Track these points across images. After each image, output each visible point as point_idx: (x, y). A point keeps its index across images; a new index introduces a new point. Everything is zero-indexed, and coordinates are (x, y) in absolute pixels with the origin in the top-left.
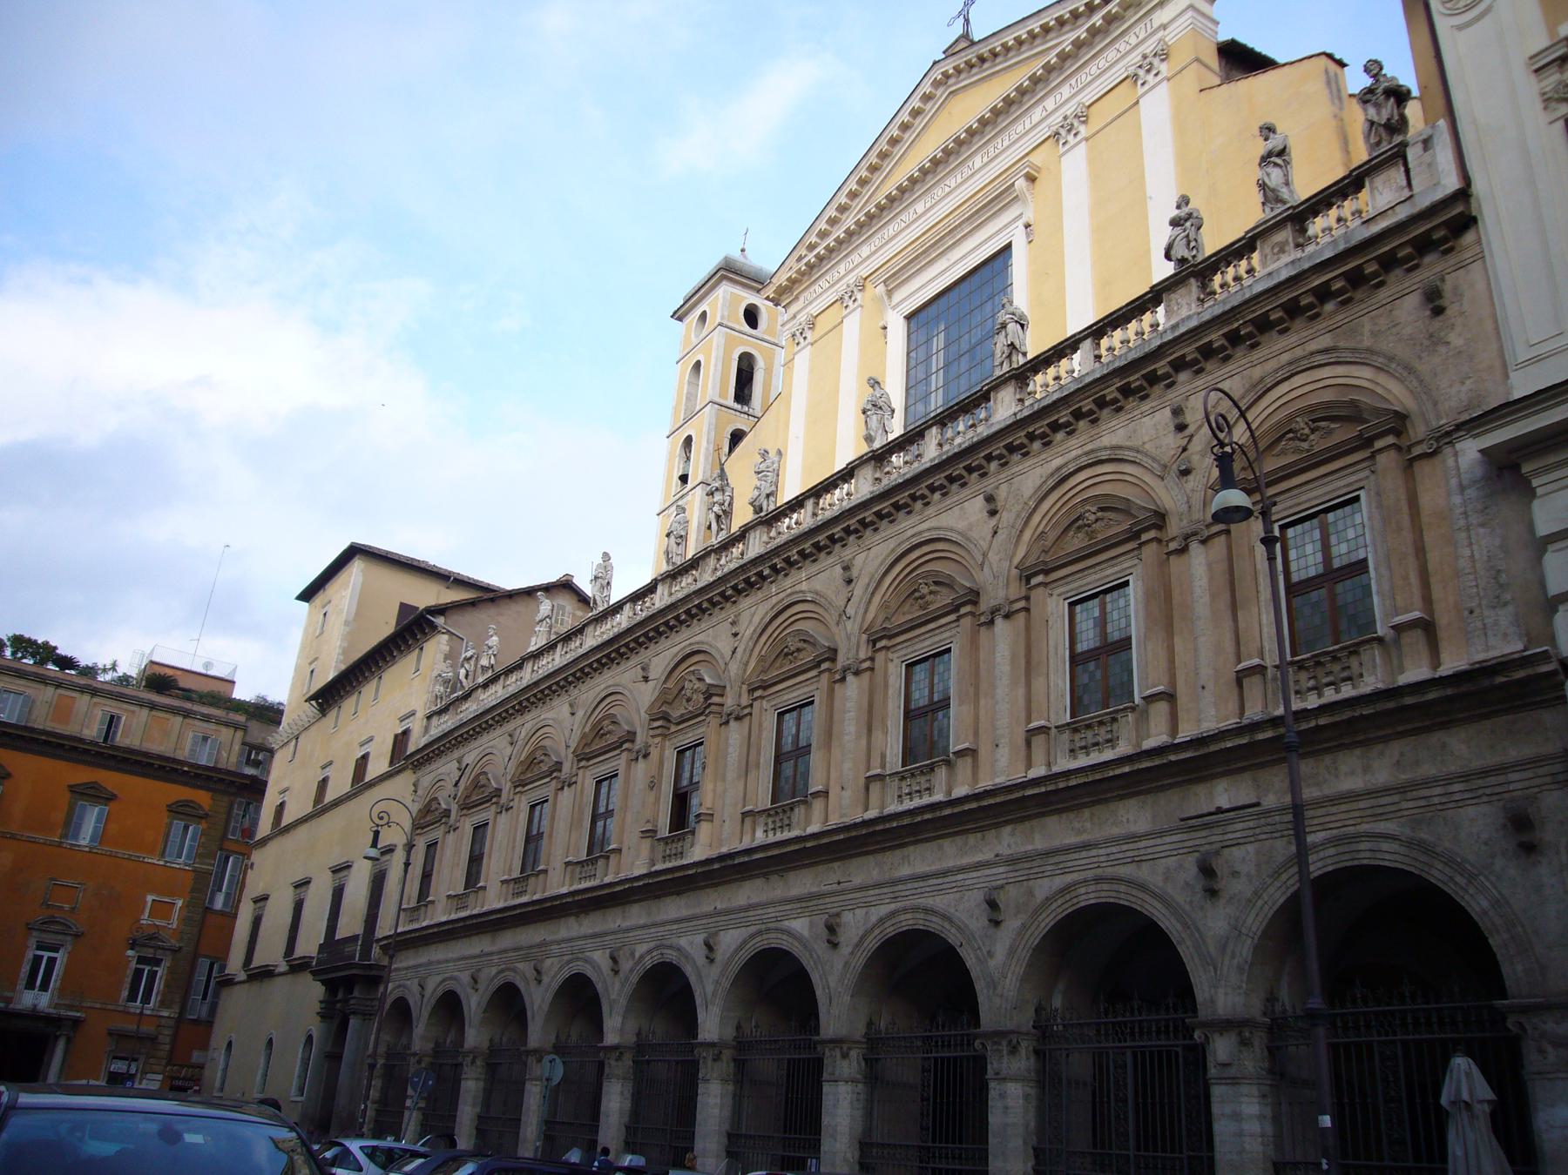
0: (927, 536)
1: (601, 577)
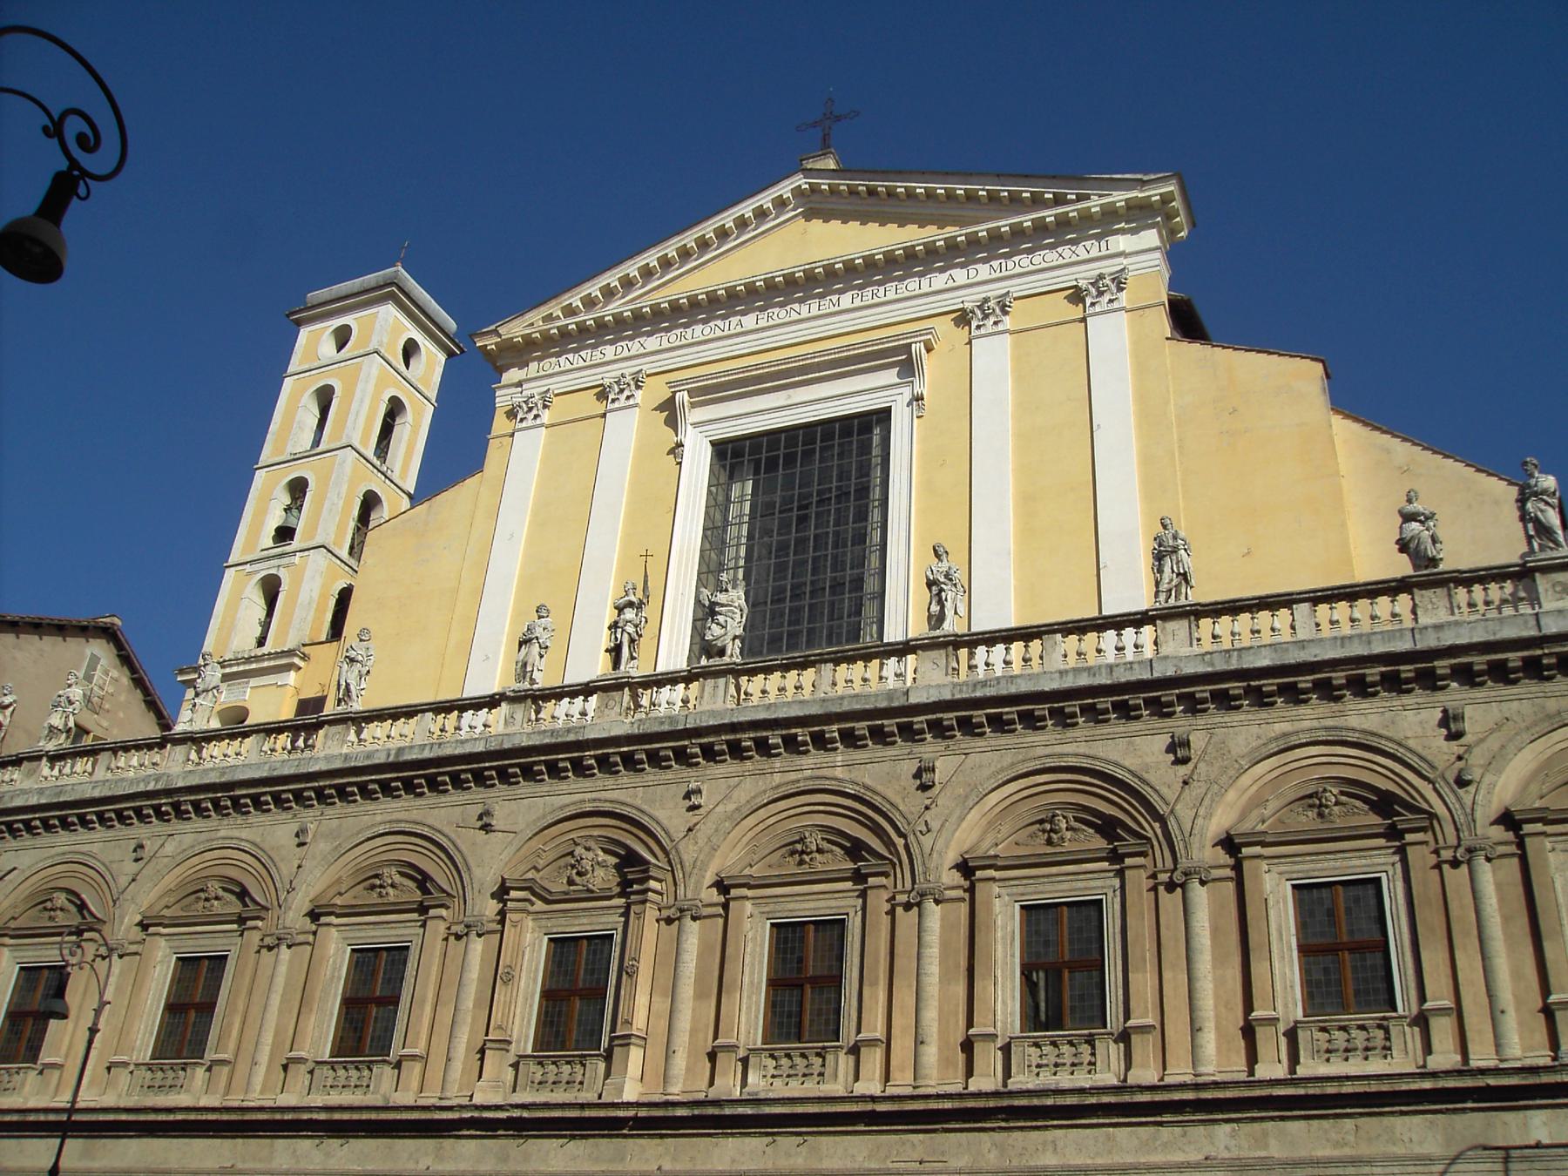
0: (1072, 761)
1: (361, 662)
